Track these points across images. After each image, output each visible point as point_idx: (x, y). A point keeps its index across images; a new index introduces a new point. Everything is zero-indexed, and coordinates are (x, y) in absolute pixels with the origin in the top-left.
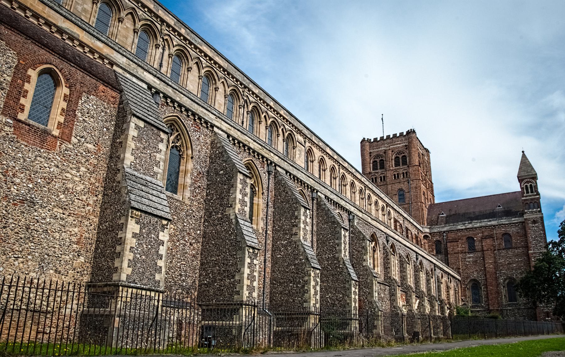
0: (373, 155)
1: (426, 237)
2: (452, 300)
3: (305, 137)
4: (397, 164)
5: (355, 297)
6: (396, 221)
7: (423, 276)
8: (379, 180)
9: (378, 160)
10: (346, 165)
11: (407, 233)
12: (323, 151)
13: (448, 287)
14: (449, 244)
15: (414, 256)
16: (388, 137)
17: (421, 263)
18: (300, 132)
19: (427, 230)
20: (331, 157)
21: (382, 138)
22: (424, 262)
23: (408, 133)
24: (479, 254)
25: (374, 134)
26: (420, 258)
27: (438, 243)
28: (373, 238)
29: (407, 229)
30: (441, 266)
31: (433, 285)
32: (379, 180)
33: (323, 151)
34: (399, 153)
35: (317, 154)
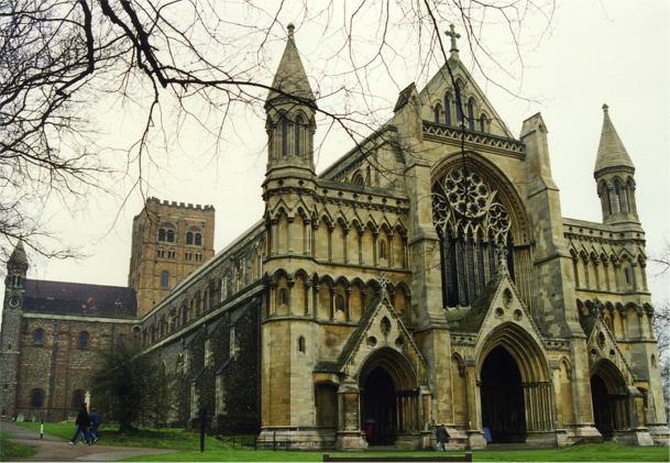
4: (189, 241)
8: (166, 255)
23: (206, 207)
32: (166, 255)
34: (194, 228)
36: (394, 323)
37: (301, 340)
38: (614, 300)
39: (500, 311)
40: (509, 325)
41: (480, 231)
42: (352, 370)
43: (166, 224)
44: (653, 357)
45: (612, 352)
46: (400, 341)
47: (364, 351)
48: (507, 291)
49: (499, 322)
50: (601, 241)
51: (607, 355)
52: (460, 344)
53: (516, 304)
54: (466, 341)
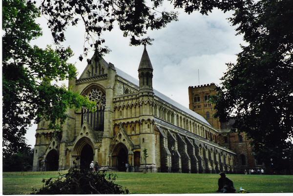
0: (195, 94)
1: (220, 135)
2: (232, 164)
3: (176, 111)
5: (198, 166)
6: (206, 131)
7: (217, 156)
9: (197, 97)
10: (188, 116)
11: (211, 135)
12: (181, 114)
13: (229, 159)
14: (231, 139)
15: (213, 148)
16: (202, 86)
17: (217, 151)
18: (175, 110)
19: (220, 132)
20: (183, 115)
21: (199, 86)
22: (218, 150)
24: (244, 143)
25: (195, 84)
26: (216, 149)
27: (226, 138)
28: (200, 145)
29: (211, 133)
30: (226, 150)
31: (222, 158)
33: (181, 114)
35: (179, 115)
36: (56, 142)
37: (36, 150)
38: (134, 120)
39: (82, 134)
40: (84, 137)
41: (98, 107)
42: (45, 156)
43: (197, 95)
44: (143, 139)
45: (124, 140)
46: (57, 147)
47: (48, 151)
48: (85, 127)
49: (81, 137)
50: (132, 99)
51: (122, 142)
52: (69, 146)
53: (87, 130)
54: (71, 144)
